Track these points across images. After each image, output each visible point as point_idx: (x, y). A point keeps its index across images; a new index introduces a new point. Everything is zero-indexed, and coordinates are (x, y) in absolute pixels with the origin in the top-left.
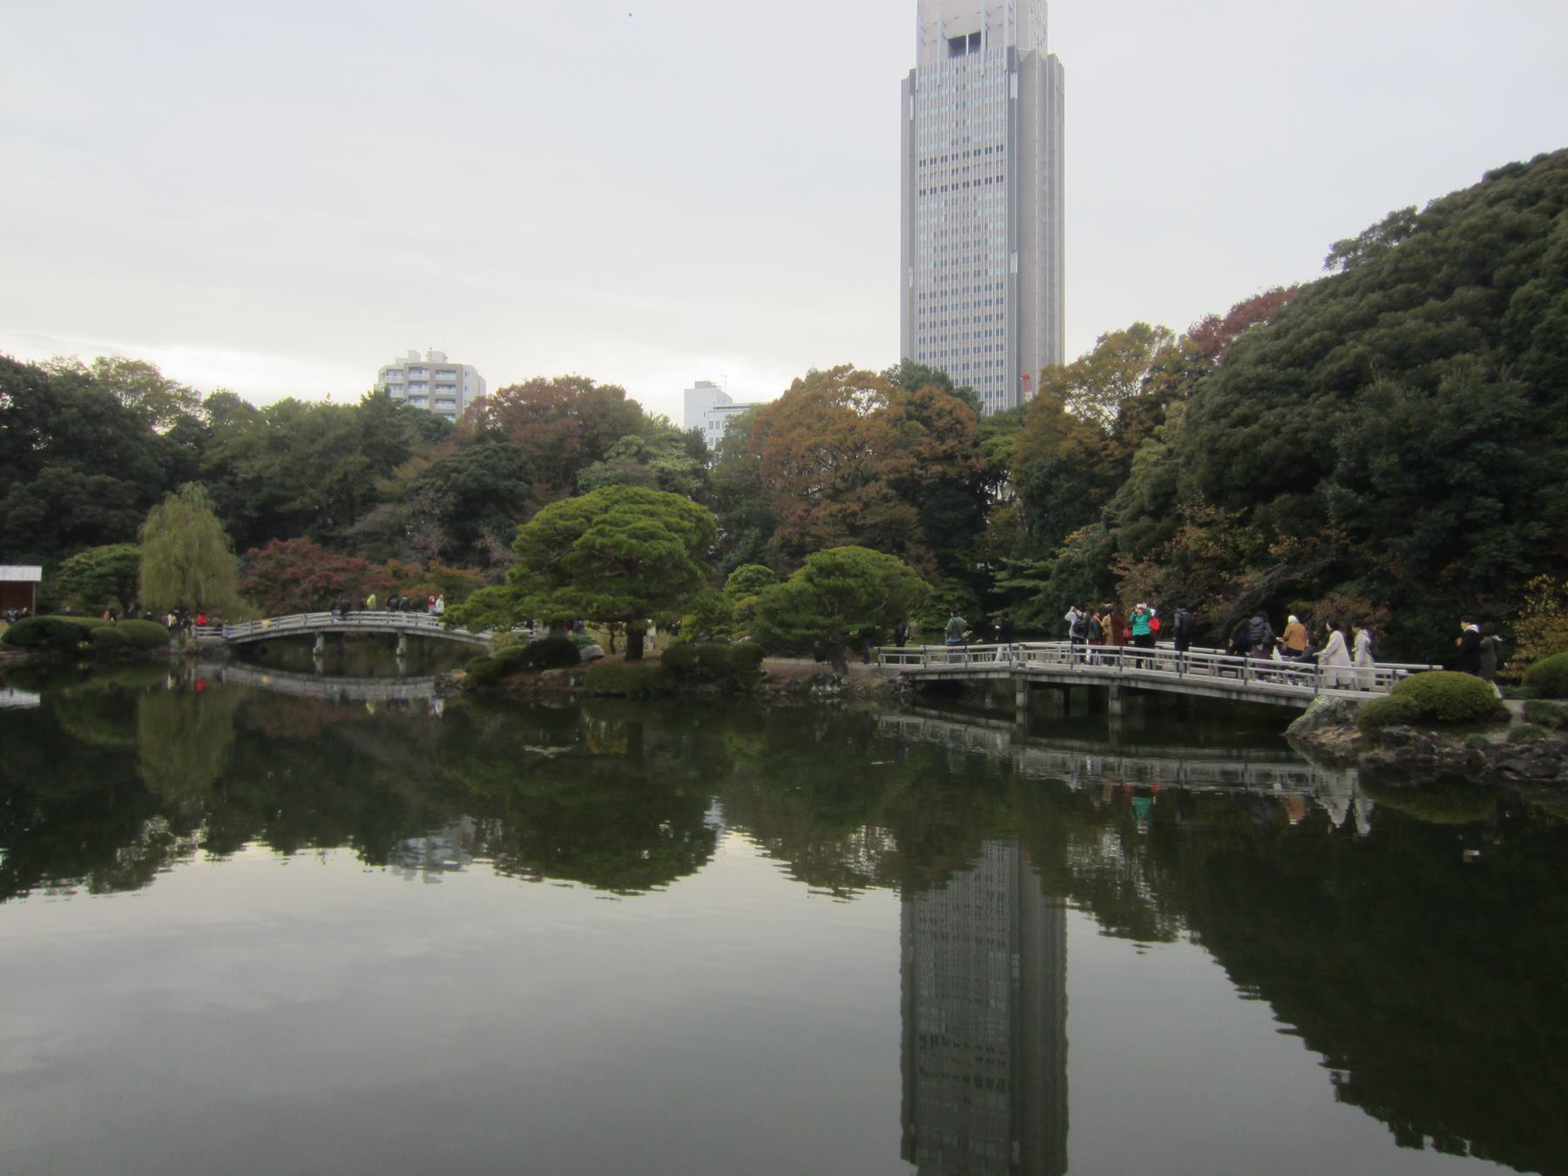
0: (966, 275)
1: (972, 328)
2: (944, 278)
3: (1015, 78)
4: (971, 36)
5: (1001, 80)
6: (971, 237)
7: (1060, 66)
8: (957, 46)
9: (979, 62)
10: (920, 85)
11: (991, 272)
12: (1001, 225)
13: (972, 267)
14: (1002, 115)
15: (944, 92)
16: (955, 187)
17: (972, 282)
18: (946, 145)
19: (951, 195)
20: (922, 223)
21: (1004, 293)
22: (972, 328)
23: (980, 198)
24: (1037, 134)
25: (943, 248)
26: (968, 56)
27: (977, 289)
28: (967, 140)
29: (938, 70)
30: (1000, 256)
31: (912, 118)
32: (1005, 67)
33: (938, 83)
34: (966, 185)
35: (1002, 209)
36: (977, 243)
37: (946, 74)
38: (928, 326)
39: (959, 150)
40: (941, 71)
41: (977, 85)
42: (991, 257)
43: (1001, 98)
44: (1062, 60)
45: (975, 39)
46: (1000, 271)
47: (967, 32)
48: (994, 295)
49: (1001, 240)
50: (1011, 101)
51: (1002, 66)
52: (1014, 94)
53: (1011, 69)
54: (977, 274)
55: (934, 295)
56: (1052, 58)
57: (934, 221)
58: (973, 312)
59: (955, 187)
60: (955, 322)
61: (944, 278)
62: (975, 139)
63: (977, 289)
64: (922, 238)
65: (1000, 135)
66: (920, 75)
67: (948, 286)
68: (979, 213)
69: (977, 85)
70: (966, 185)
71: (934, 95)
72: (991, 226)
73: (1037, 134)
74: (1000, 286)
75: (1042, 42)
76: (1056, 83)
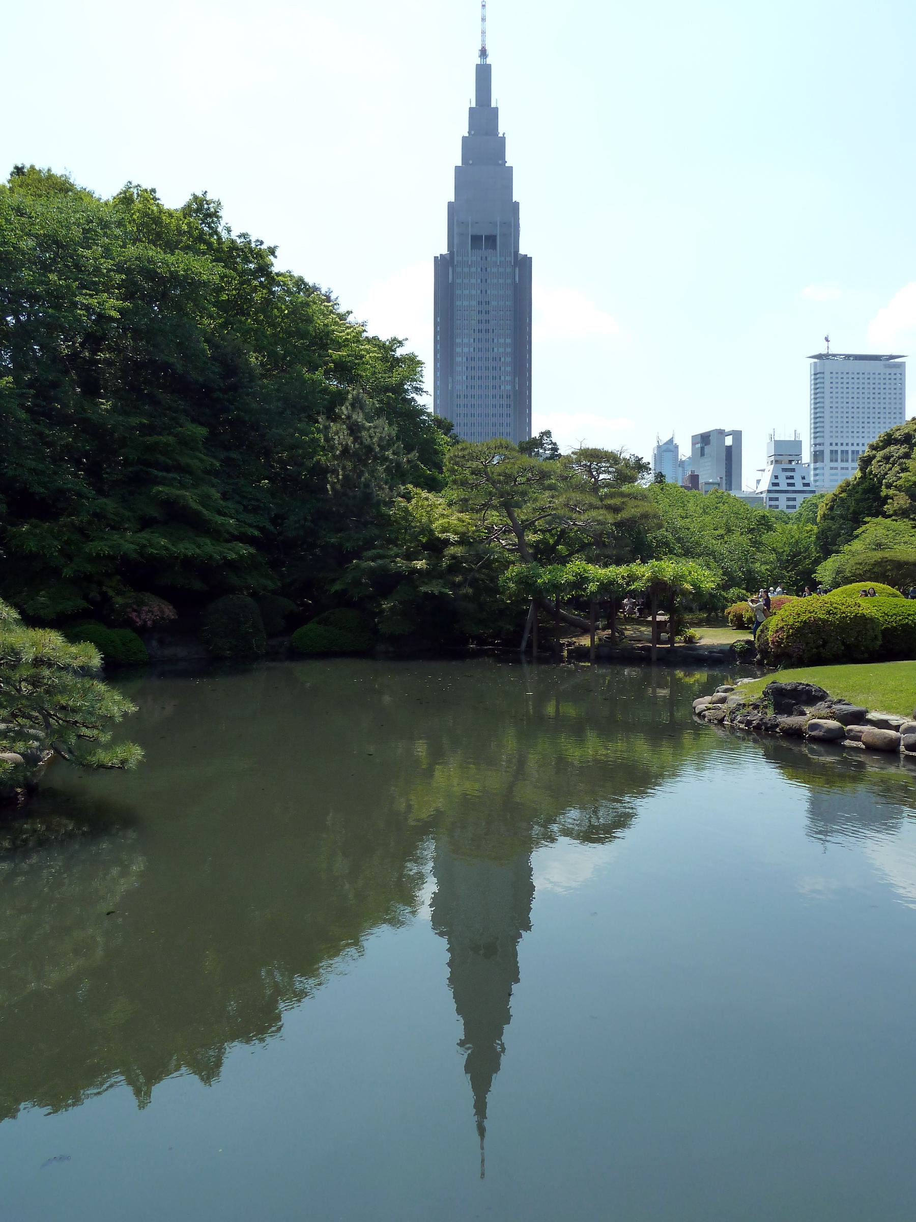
0: (487, 387)
5: (509, 270)
8: (476, 239)
9: (496, 256)
10: (457, 262)
11: (502, 387)
12: (509, 359)
15: (473, 270)
16: (480, 331)
18: (474, 303)
20: (458, 350)
25: (473, 368)
28: (488, 303)
29: (470, 255)
32: (513, 264)
33: (470, 263)
34: (487, 331)
35: (509, 350)
37: (474, 259)
41: (494, 270)
43: (509, 281)
46: (508, 387)
47: (484, 233)
49: (509, 369)
51: (510, 262)
53: (515, 266)
54: (494, 387)
55: (466, 396)
57: (466, 350)
59: (480, 331)
61: (473, 387)
62: (494, 303)
64: (459, 359)
68: (495, 350)
69: (494, 270)
70: (487, 331)
71: (466, 270)
72: (503, 359)
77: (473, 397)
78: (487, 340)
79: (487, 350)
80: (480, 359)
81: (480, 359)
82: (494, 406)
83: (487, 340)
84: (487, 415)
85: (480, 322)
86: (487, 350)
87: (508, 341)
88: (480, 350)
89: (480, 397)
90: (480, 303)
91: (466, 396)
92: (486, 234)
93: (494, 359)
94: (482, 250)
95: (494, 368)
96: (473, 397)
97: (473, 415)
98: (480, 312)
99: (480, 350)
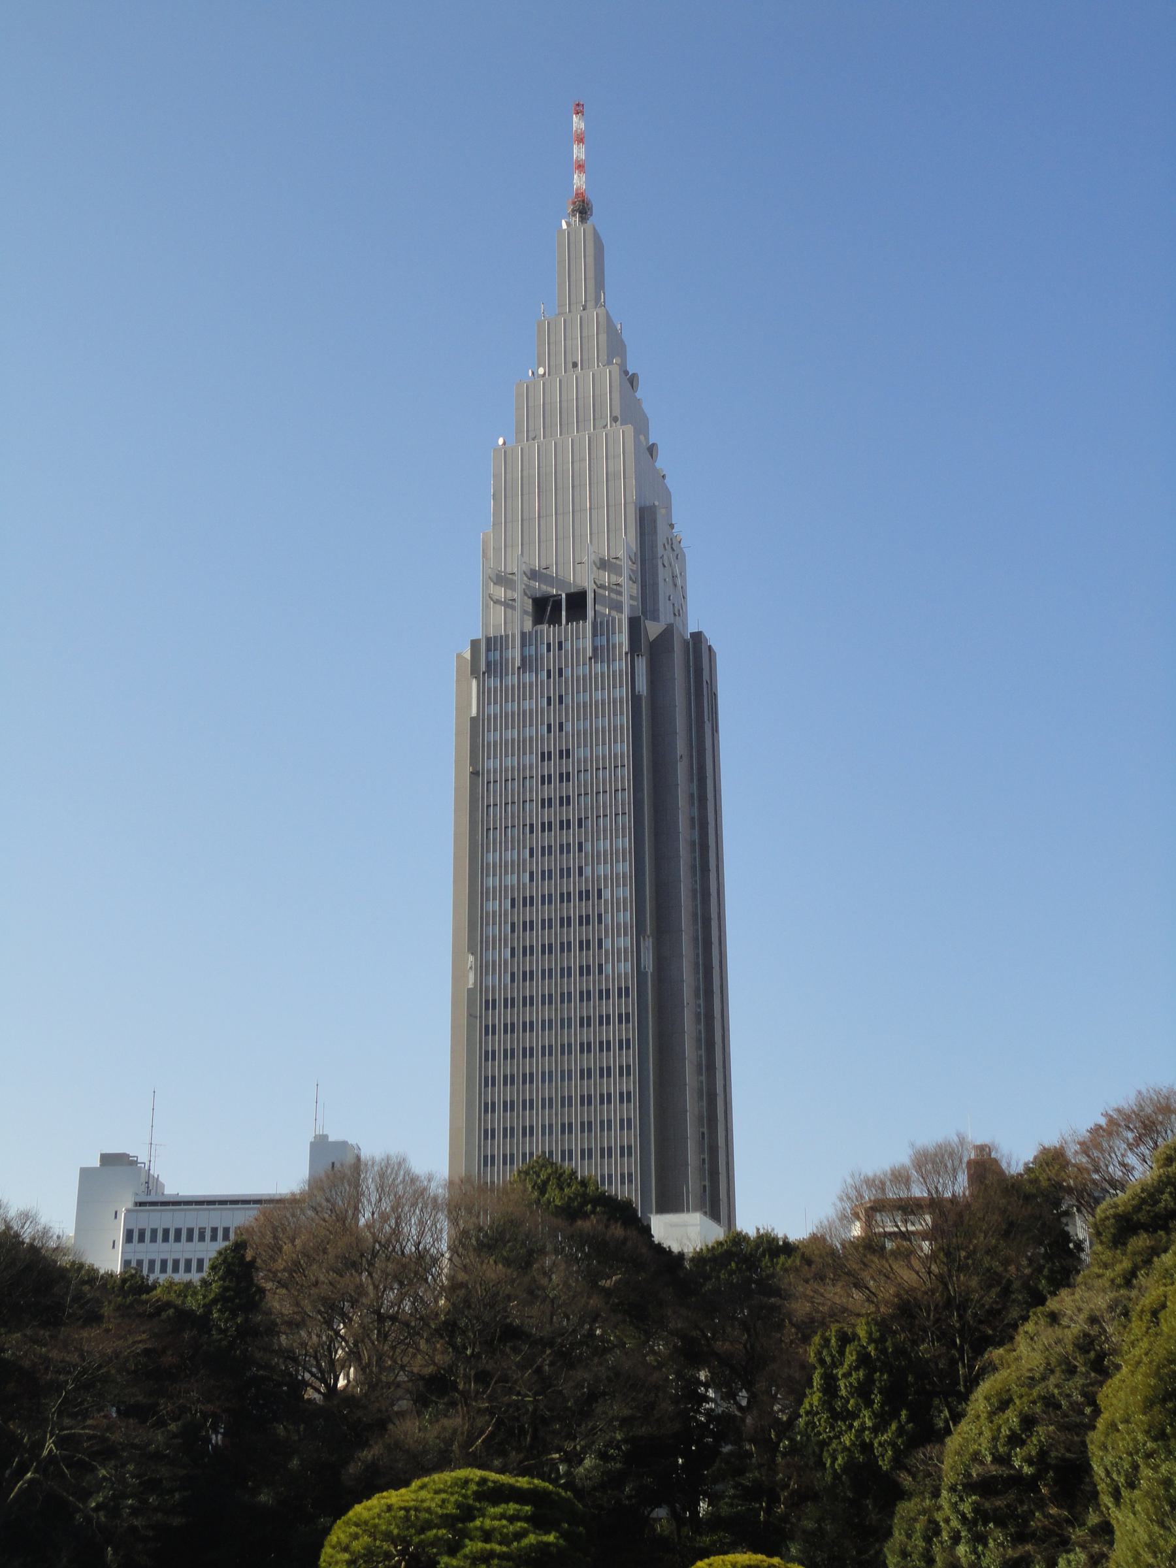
1: (577, 1062)
2: (528, 976)
3: (642, 664)
4: (567, 595)
6: (575, 909)
7: (710, 647)
12: (625, 892)
13: (575, 959)
14: (624, 720)
16: (547, 827)
17: (575, 984)
18: (532, 759)
19: (539, 839)
21: (630, 1005)
22: (577, 1062)
23: (588, 847)
24: (681, 747)
25: (529, 926)
26: (566, 628)
27: (585, 996)
28: (565, 754)
30: (625, 942)
31: (474, 713)
32: (625, 648)
34: (565, 825)
35: (625, 867)
36: (585, 920)
38: (500, 1055)
39: (552, 768)
40: (523, 645)
42: (608, 944)
43: (622, 692)
44: (713, 639)
45: (577, 602)
46: (626, 967)
48: (612, 1007)
49: (626, 917)
50: (636, 699)
52: (642, 686)
54: (585, 970)
55: (510, 1003)
56: (698, 637)
57: (511, 880)
58: (577, 1035)
59: (547, 827)
60: (547, 1051)
61: (528, 976)
62: (580, 753)
63: (585, 996)
65: (624, 748)
66: (488, 650)
67: (537, 988)
68: (588, 871)
70: (565, 825)
72: (607, 894)
73: (681, 747)
74: (623, 992)
75: (679, 612)
76: (706, 676)
77: (529, 1001)
78: (565, 849)
79: (566, 873)
80: (547, 899)
81: (547, 899)
82: (585, 1022)
83: (565, 849)
84: (566, 1049)
85: (546, 803)
86: (566, 873)
87: (625, 843)
88: (547, 875)
89: (548, 999)
90: (545, 757)
91: (510, 1003)
92: (569, 592)
93: (584, 895)
94: (560, 625)
95: (585, 920)
96: (529, 1001)
97: (528, 1052)
98: (545, 780)
99: (547, 875)
